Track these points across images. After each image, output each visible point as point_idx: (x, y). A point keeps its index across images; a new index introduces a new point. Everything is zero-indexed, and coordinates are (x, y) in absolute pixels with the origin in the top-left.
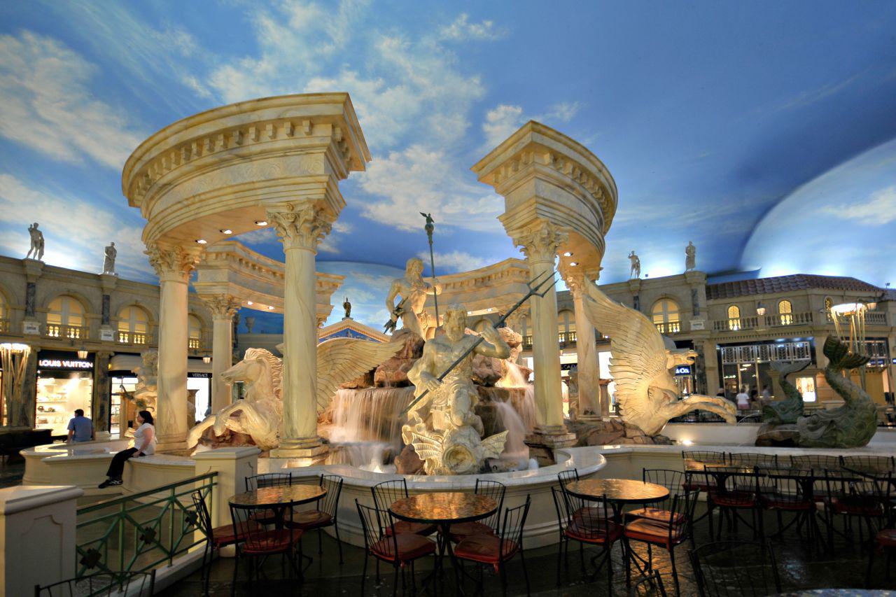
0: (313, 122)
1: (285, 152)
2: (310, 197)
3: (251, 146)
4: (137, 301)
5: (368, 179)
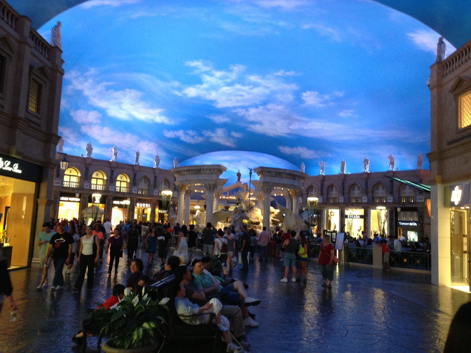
0: (214, 169)
1: (208, 174)
3: (202, 172)
4: (145, 175)
5: (249, 116)
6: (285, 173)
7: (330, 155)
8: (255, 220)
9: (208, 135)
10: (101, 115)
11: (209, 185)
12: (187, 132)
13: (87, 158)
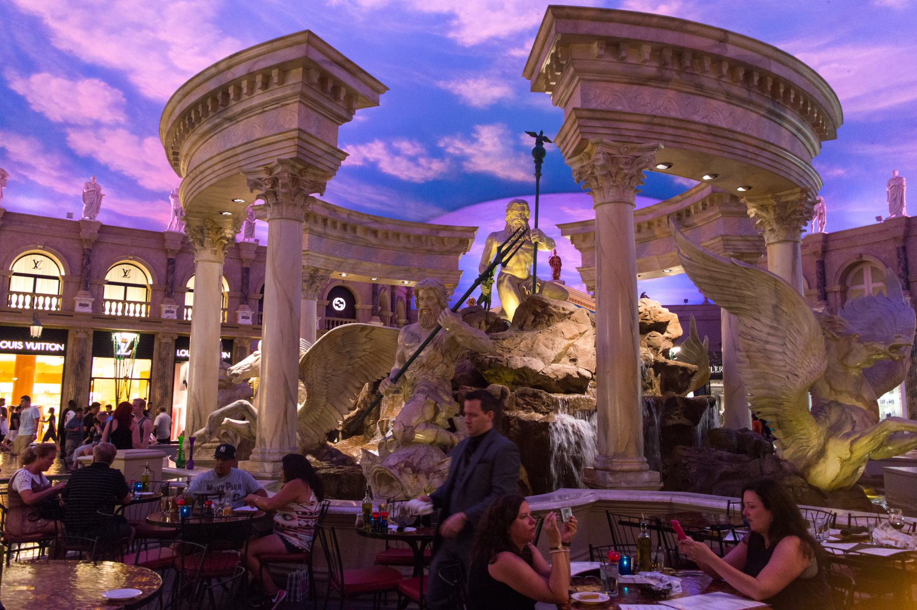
2: (279, 157)
6: (718, 60)
7: (839, 172)
8: (555, 366)
9: (457, 152)
10: (115, 95)
11: (270, 171)
12: (396, 145)
13: (83, 221)
